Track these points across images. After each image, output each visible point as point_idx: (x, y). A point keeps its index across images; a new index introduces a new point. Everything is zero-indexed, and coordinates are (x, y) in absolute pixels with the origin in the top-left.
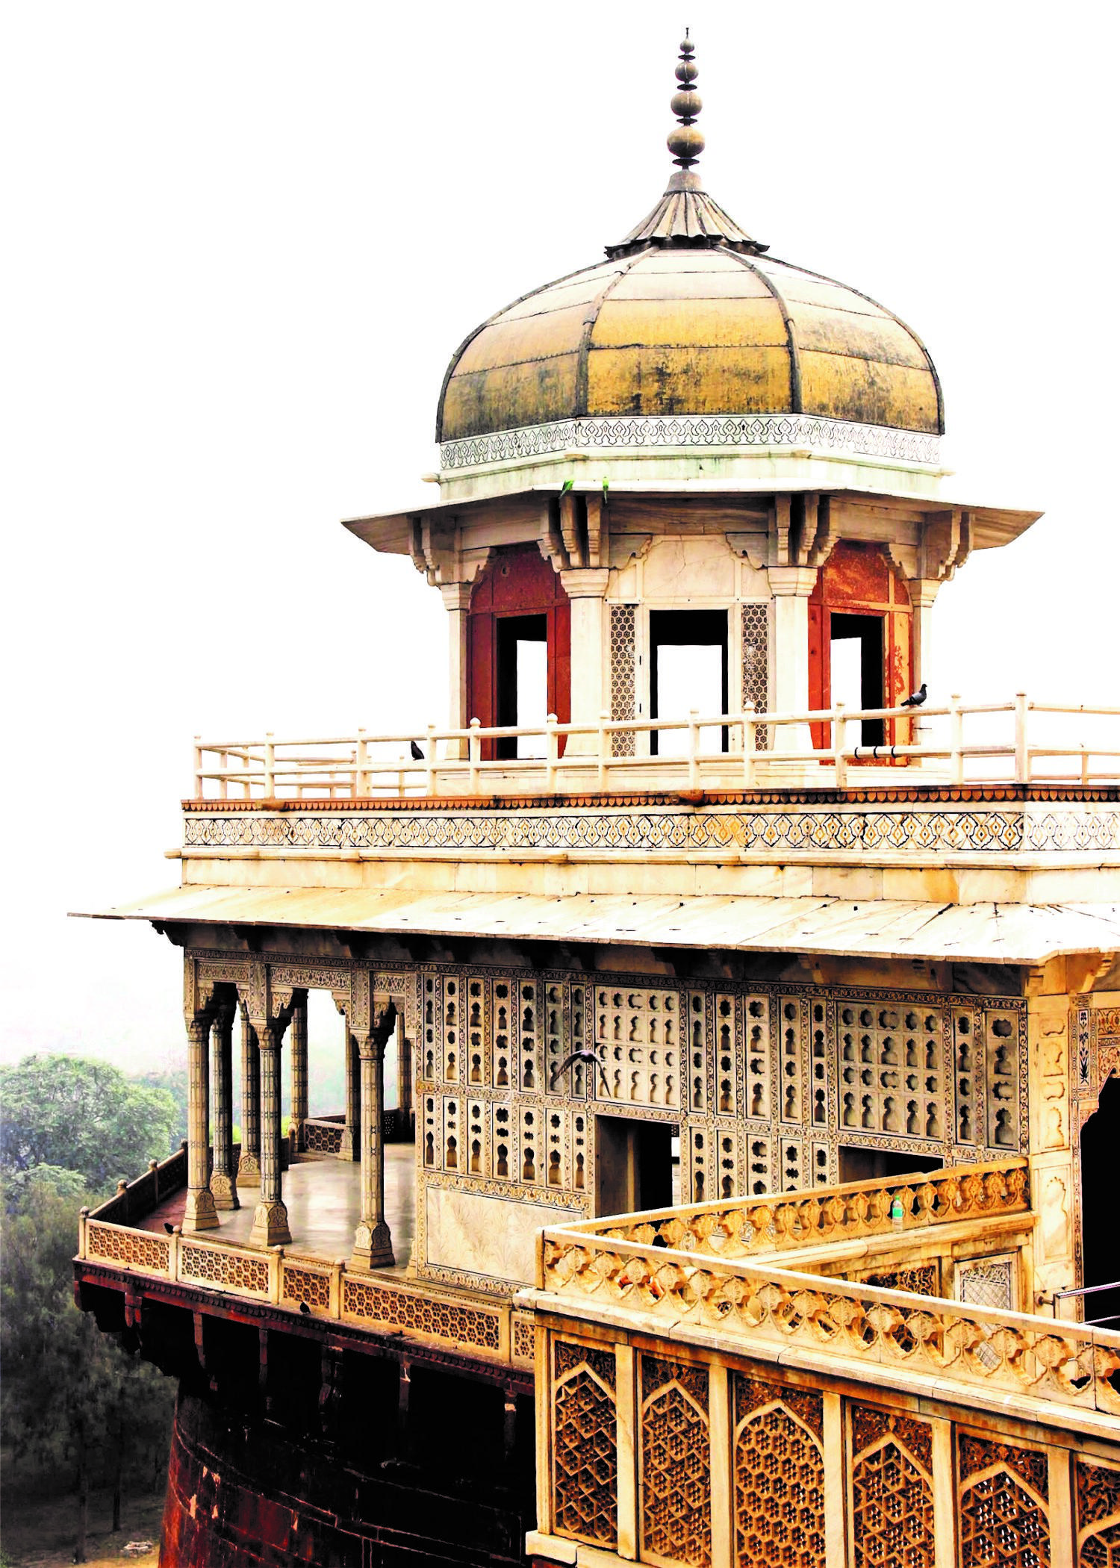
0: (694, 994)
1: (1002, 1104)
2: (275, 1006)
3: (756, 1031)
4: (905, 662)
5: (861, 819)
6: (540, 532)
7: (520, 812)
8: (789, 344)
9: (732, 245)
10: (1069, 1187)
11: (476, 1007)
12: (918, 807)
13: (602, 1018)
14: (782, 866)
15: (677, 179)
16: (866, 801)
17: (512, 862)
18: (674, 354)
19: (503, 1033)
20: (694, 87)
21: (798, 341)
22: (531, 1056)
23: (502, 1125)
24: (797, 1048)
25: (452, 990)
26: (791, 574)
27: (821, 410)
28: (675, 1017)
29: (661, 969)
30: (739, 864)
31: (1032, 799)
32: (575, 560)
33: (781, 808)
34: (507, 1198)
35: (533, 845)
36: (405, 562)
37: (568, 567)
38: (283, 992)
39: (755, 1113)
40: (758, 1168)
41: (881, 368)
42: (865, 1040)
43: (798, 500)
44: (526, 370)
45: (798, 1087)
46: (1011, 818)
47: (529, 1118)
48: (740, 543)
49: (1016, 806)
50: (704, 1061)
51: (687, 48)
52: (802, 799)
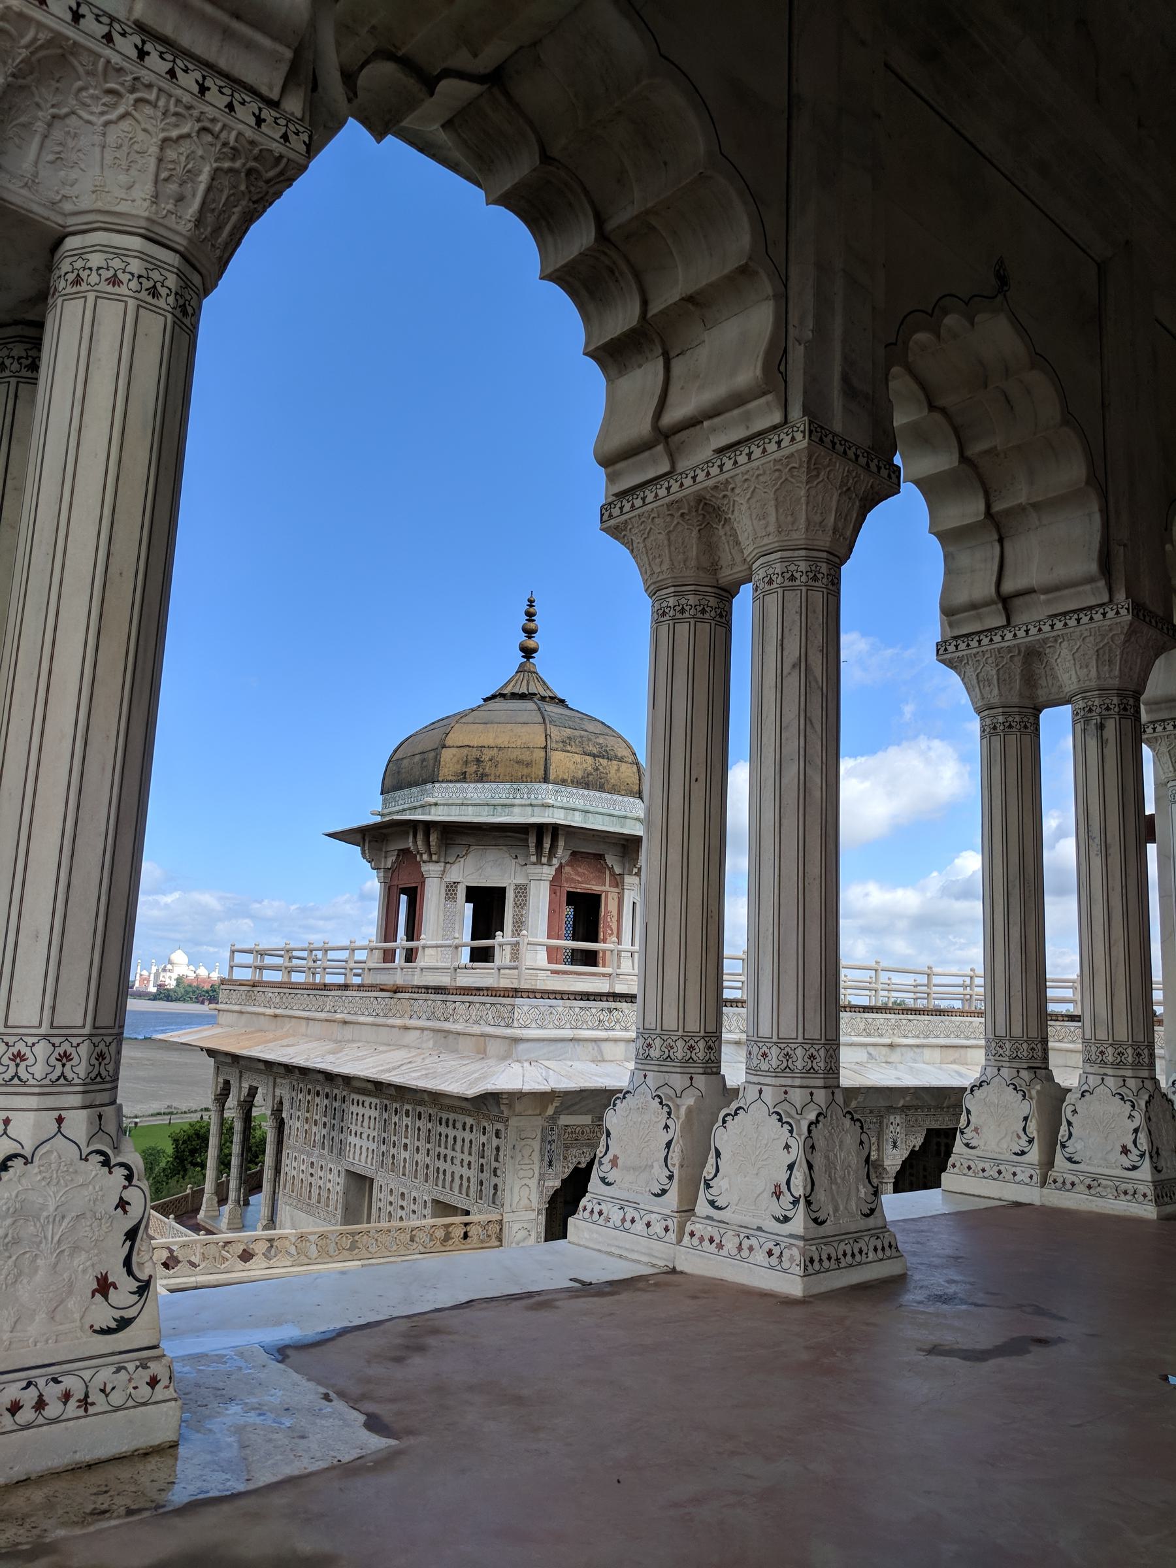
0: (386, 1102)
1: (495, 1180)
3: (407, 1126)
7: (332, 993)
8: (546, 747)
9: (543, 698)
10: (533, 1234)
18: (486, 751)
26: (537, 869)
27: (563, 782)
32: (425, 857)
34: (308, 1213)
38: (246, 1085)
40: (402, 1208)
41: (604, 762)
42: (447, 1136)
43: (540, 829)
44: (417, 758)
46: (510, 1008)
48: (515, 851)
51: (531, 603)
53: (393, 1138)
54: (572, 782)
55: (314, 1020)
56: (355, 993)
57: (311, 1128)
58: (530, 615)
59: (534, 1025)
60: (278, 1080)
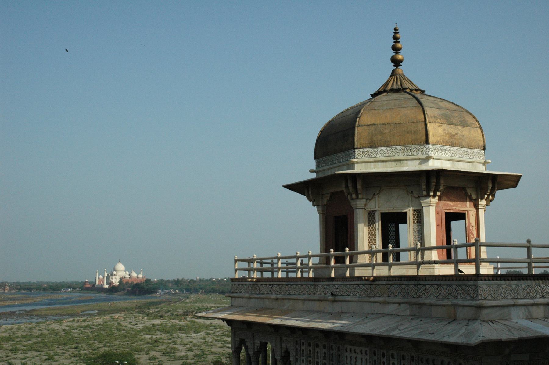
2: (256, 347)
4: (474, 228)
6: (343, 188)
7: (321, 283)
9: (411, 90)
12: (443, 283)
13: (347, 357)
14: (399, 304)
15: (393, 71)
16: (426, 280)
17: (319, 300)
19: (318, 360)
28: (368, 357)
30: (386, 303)
31: (481, 280)
32: (354, 196)
33: (398, 282)
35: (325, 294)
36: (304, 198)
37: (353, 199)
38: (258, 342)
46: (473, 287)
49: (475, 283)
52: (406, 279)
54: (443, 142)
55: (309, 300)
56: (339, 283)
58: (396, 38)
59: (490, 298)
60: (284, 338)
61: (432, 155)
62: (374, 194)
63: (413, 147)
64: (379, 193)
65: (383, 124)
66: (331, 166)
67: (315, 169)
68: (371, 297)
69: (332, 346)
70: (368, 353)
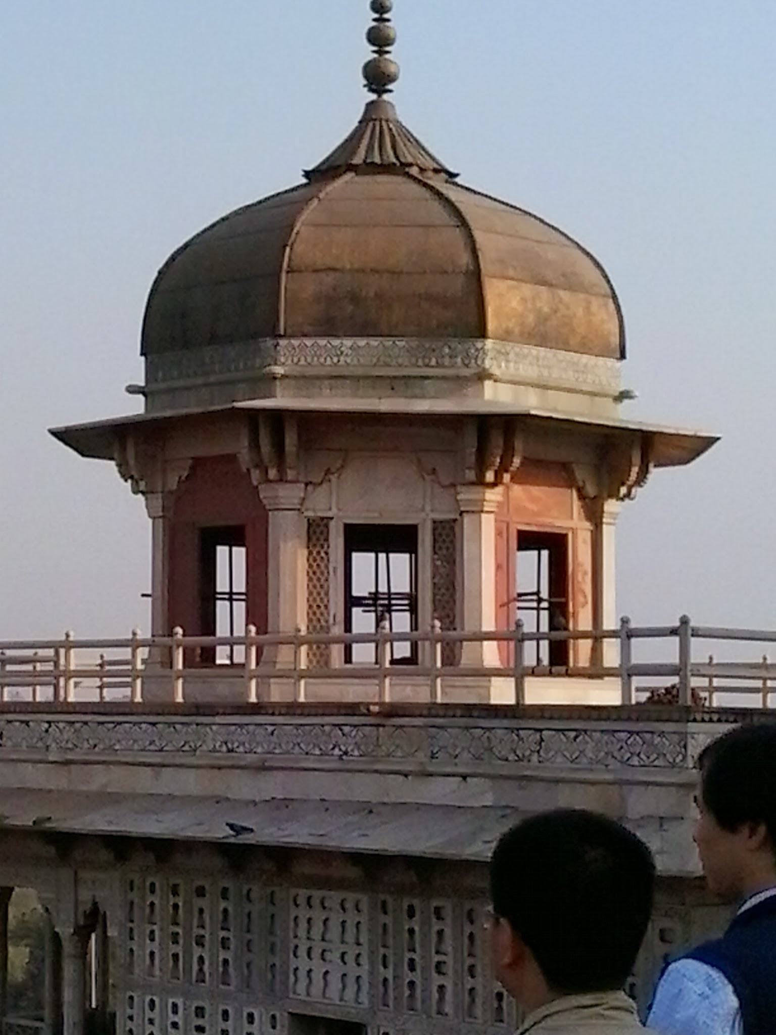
0: (382, 897)
5: (538, 736)
7: (218, 719)
11: (176, 906)
13: (296, 918)
14: (464, 777)
16: (542, 717)
17: (213, 767)
19: (202, 932)
20: (388, 20)
21: (483, 271)
22: (229, 956)
23: (200, 1022)
24: (478, 951)
25: (153, 891)
28: (364, 919)
29: (353, 872)
31: (695, 720)
32: (272, 473)
35: (230, 751)
39: (439, 1013)
41: (564, 295)
45: (480, 990)
47: (225, 1014)
50: (391, 960)
53: (408, 955)
54: (522, 334)
57: (188, 952)
61: (495, 371)
62: (328, 472)
63: (440, 344)
64: (342, 467)
65: (358, 271)
66: (200, 381)
67: (142, 383)
68: (376, 760)
69: (249, 891)
70: (364, 906)
